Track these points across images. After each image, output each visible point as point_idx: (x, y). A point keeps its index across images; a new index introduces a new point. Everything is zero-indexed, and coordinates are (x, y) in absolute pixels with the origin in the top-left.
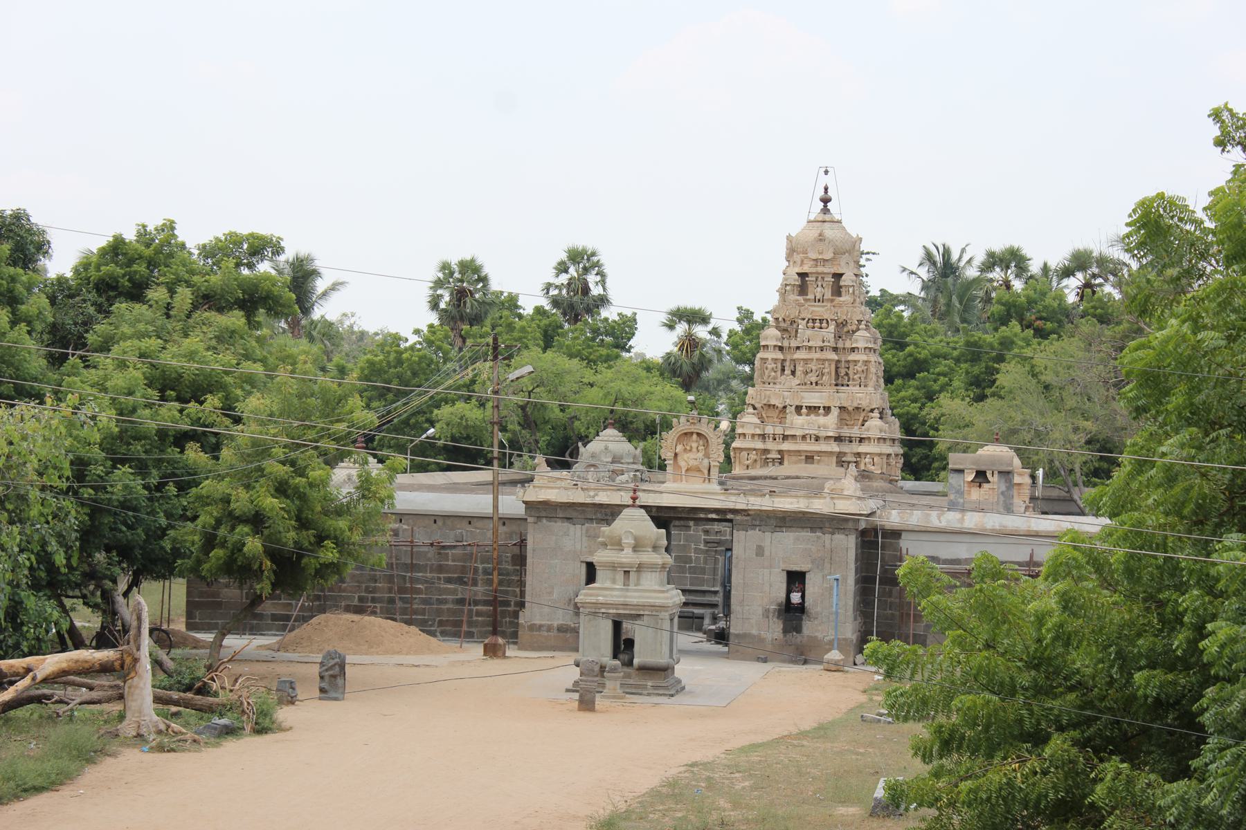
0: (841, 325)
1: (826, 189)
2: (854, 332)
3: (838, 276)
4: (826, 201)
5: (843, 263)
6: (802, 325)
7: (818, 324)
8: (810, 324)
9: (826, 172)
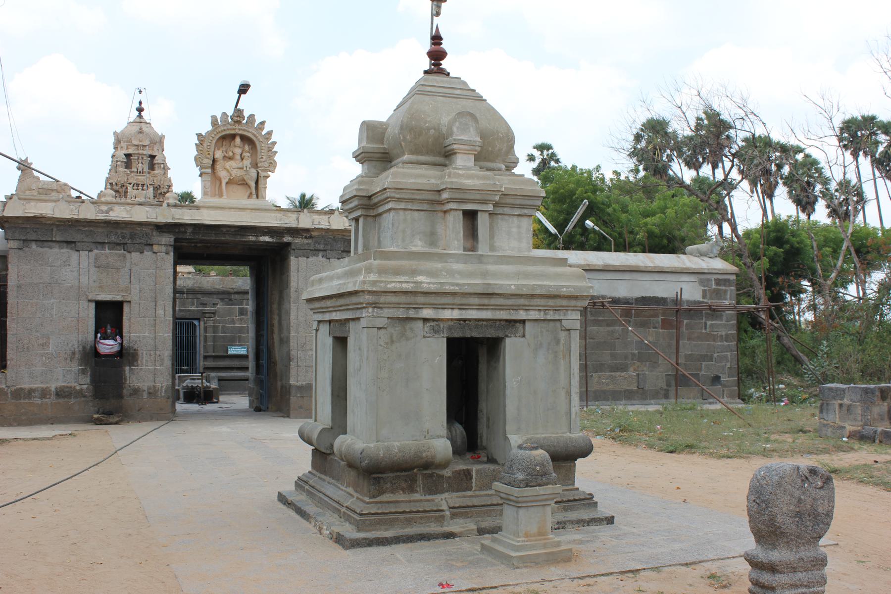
0: (156, 188)
1: (140, 103)
2: (165, 193)
3: (153, 157)
4: (140, 110)
5: (155, 149)
6: (130, 188)
7: (140, 187)
8: (135, 187)
9: (140, 92)
